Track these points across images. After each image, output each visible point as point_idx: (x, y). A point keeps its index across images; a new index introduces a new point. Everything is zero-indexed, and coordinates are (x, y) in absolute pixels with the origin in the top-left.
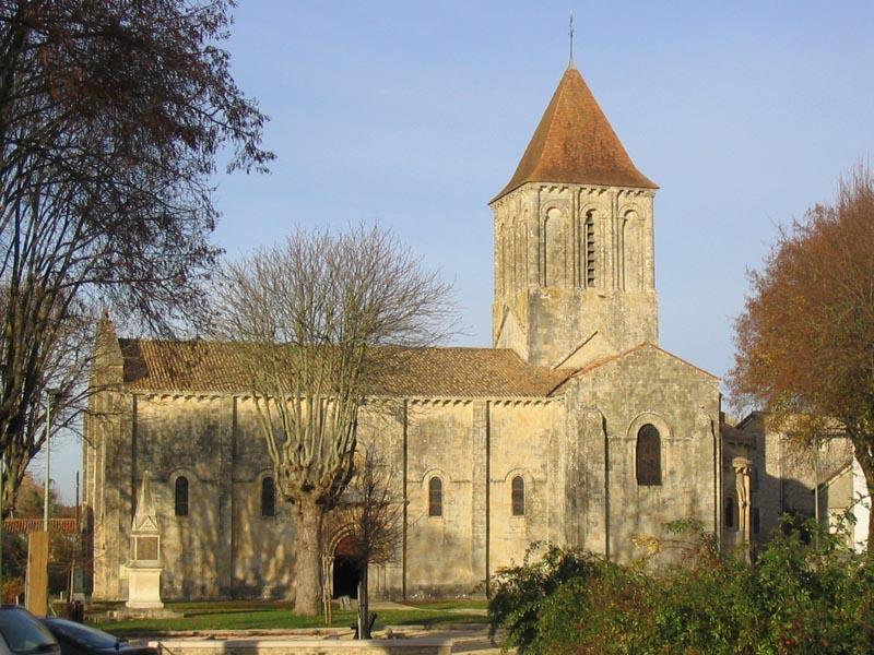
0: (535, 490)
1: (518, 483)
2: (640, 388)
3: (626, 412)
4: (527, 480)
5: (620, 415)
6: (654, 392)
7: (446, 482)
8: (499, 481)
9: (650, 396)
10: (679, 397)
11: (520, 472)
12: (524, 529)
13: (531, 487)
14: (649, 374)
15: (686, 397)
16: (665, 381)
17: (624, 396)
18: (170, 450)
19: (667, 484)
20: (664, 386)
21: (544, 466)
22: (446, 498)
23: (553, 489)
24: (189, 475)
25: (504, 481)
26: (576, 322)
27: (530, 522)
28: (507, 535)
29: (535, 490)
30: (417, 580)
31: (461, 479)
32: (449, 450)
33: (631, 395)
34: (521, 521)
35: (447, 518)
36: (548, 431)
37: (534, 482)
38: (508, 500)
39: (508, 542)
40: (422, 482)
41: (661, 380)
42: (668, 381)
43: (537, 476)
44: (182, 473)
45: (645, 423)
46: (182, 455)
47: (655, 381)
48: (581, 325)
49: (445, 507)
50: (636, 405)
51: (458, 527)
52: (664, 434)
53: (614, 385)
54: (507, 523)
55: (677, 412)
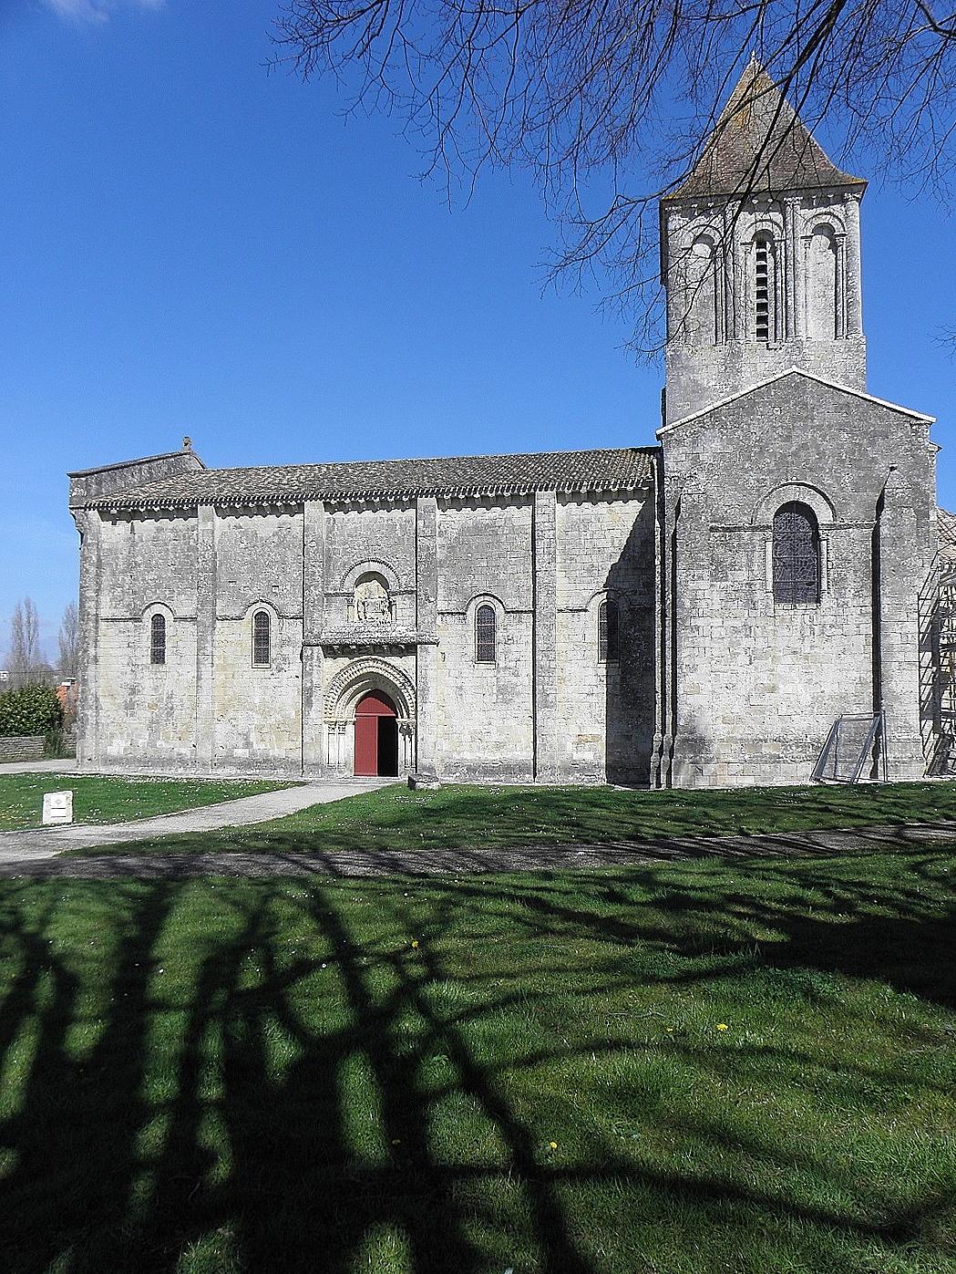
0: (632, 623)
2: (779, 443)
6: (804, 446)
7: (499, 611)
9: (795, 454)
13: (628, 616)
15: (864, 453)
19: (826, 600)
22: (499, 635)
24: (164, 611)
29: (632, 623)
40: (464, 614)
45: (786, 500)
46: (158, 586)
47: (804, 429)
49: (499, 649)
50: (771, 472)
52: (824, 515)
53: (730, 441)
54: (591, 671)
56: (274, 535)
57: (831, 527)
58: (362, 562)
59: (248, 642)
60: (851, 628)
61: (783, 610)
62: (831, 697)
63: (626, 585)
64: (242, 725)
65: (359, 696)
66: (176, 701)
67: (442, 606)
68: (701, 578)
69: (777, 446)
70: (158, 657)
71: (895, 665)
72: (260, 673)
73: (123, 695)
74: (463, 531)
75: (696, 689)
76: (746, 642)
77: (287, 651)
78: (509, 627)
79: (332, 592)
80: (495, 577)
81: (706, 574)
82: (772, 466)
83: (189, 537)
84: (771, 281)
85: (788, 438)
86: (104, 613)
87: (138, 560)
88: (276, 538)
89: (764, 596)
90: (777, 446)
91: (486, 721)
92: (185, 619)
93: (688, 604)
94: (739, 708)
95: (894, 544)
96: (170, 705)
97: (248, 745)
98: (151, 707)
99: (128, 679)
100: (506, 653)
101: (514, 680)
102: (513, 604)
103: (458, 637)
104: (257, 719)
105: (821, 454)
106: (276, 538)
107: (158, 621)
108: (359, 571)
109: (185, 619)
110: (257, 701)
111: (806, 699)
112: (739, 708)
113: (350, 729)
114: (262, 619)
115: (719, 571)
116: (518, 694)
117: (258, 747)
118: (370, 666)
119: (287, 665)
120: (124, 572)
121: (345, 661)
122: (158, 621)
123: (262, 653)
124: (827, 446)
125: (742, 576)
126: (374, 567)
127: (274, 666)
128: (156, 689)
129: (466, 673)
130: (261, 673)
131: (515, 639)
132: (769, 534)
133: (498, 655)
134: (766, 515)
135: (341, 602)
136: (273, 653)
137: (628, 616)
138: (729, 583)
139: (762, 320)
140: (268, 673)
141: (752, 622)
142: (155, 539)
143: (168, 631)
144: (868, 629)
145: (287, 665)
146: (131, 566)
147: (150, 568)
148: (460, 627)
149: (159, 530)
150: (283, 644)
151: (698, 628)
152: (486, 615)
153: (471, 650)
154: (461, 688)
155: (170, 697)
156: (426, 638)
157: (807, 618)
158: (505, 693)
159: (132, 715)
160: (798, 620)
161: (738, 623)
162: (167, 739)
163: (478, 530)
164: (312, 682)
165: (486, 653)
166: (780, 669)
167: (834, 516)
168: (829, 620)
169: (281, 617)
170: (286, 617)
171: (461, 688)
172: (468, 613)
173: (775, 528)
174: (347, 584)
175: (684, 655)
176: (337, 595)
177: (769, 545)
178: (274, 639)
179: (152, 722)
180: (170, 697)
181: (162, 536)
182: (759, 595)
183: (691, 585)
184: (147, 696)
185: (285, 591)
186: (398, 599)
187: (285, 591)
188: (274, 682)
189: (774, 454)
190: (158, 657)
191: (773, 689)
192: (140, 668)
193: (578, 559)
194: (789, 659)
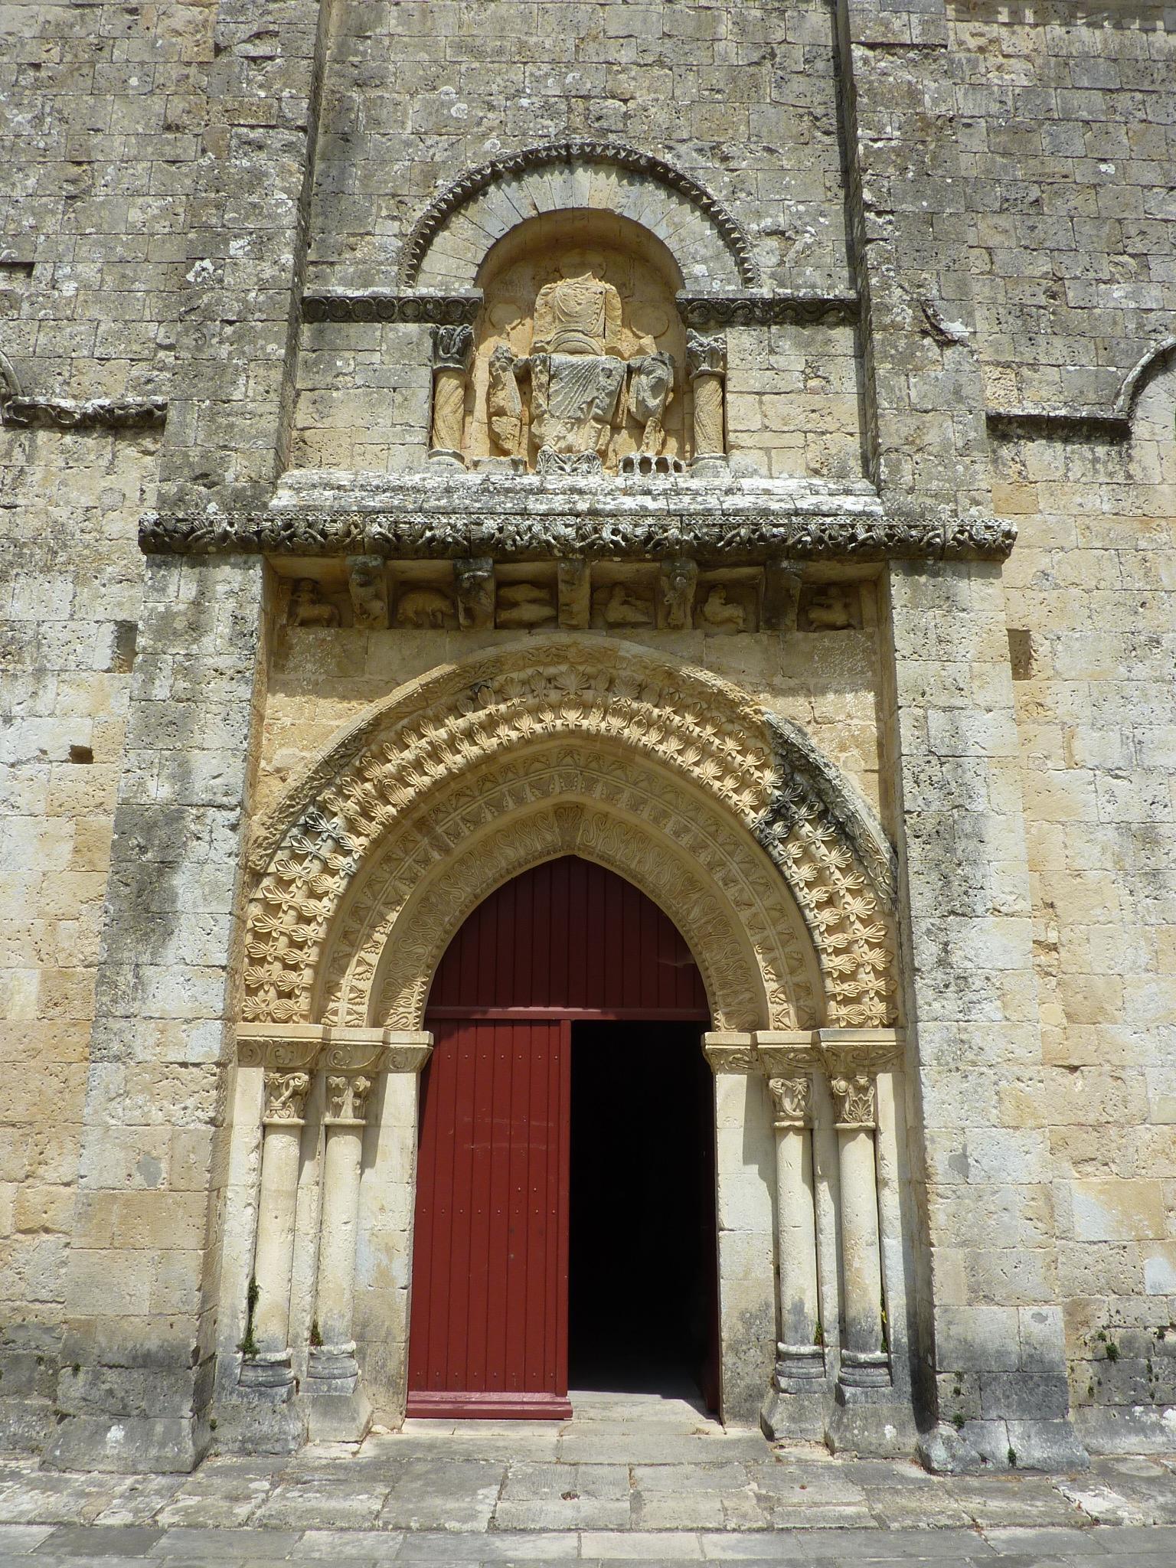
40: (1117, 432)
56: (42, 37)
145: (22, 688)
148: (1100, 501)
154: (1147, 836)
164: (183, 775)
170: (57, 420)
176: (379, 311)
186: (738, 341)
187: (69, 289)
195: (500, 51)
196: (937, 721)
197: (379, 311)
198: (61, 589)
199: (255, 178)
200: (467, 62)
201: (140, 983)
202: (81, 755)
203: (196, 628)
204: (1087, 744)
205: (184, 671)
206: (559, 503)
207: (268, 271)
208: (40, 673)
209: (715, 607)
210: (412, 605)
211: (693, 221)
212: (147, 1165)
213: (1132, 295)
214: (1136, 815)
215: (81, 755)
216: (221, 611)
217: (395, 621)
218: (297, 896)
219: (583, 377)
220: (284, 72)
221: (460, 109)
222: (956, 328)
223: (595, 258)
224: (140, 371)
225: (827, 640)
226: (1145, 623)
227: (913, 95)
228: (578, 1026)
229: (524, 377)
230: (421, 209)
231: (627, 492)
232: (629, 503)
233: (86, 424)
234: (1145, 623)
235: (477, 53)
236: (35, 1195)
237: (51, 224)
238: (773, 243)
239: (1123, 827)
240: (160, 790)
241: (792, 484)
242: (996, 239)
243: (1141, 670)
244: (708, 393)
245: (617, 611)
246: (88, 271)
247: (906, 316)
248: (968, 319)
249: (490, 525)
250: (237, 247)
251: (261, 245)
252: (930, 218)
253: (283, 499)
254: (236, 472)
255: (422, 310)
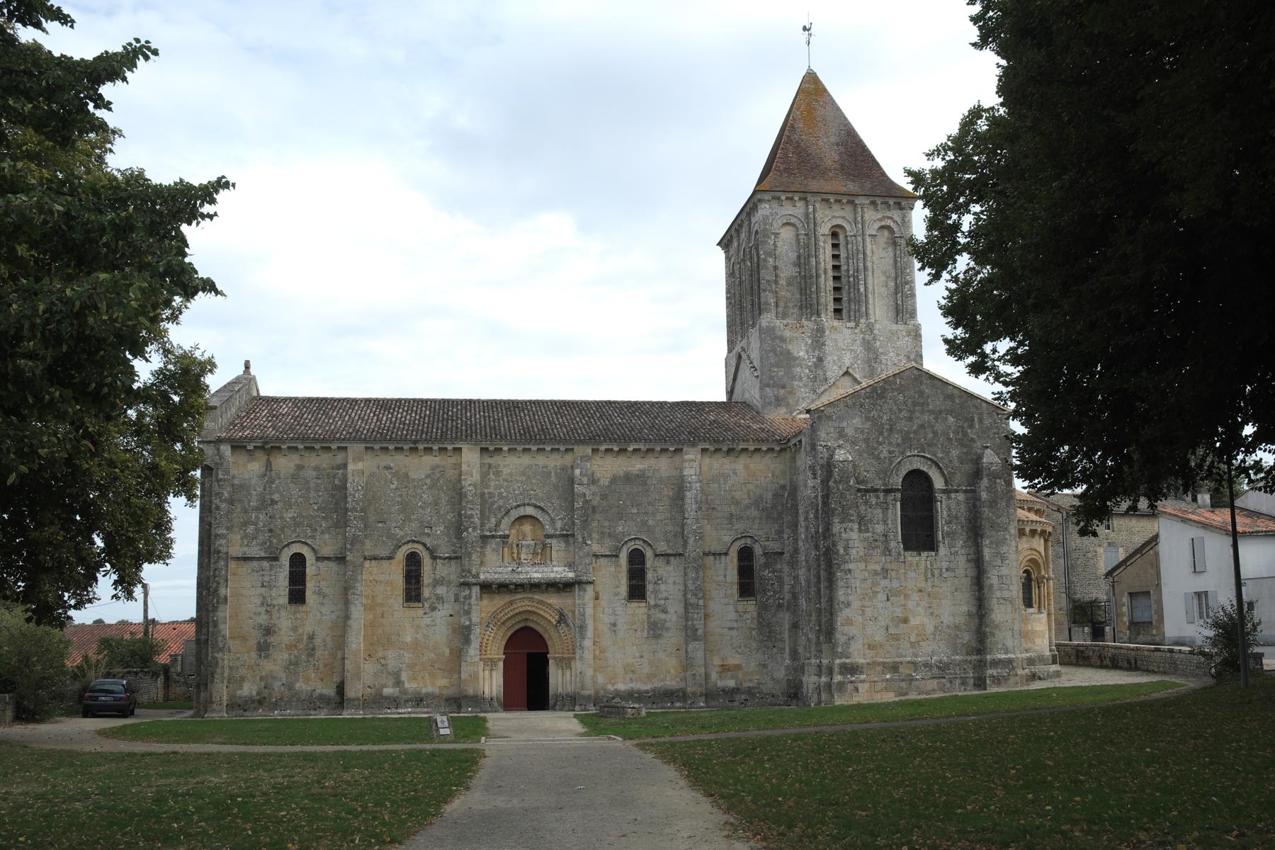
0: (766, 565)
1: (745, 555)
2: (903, 423)
3: (885, 454)
4: (758, 550)
5: (878, 458)
6: (922, 426)
7: (649, 554)
8: (720, 554)
9: (915, 432)
10: (956, 433)
11: (749, 541)
12: (755, 614)
13: (762, 560)
14: (915, 404)
15: (965, 434)
16: (937, 414)
17: (881, 433)
18: (281, 518)
19: (943, 550)
20: (936, 419)
21: (780, 532)
22: (650, 576)
23: (793, 564)
24: (306, 551)
25: (726, 554)
26: (820, 360)
27: (763, 607)
28: (735, 625)
29: (766, 565)
30: (613, 684)
31: (669, 551)
32: (654, 514)
33: (891, 430)
34: (751, 606)
35: (652, 602)
36: (783, 487)
37: (765, 554)
38: (733, 575)
39: (734, 633)
40: (617, 556)
41: (931, 412)
42: (940, 412)
43: (773, 546)
44: (297, 548)
45: (911, 469)
46: (297, 525)
47: (922, 412)
48: (825, 363)
49: (650, 587)
50: (898, 445)
51: (665, 611)
52: (938, 483)
53: (867, 419)
54: (731, 608)
55: (955, 453)
57: (944, 491)
58: (518, 506)
59: (399, 581)
60: (960, 572)
61: (911, 557)
62: (948, 627)
63: (761, 533)
64: (392, 664)
65: (509, 634)
66: (318, 641)
67: (596, 548)
68: (852, 530)
69: (902, 425)
70: (297, 596)
71: (995, 601)
72: (411, 613)
73: (255, 637)
74: (614, 480)
75: (849, 622)
76: (884, 583)
77: (441, 590)
78: (658, 569)
79: (488, 534)
80: (644, 523)
81: (856, 526)
82: (899, 441)
83: (334, 477)
84: (844, 268)
85: (910, 419)
86: (236, 551)
87: (276, 497)
88: (428, 481)
89: (896, 543)
90: (902, 425)
91: (637, 655)
92: (328, 559)
93: (842, 551)
94: (879, 637)
95: (991, 506)
96: (311, 646)
97: (398, 683)
98: (290, 647)
99: (263, 619)
100: (656, 592)
101: (663, 616)
102: (662, 547)
103: (613, 578)
104: (408, 657)
105: (935, 433)
106: (428, 481)
107: (298, 562)
108: (515, 514)
109: (328, 559)
110: (408, 639)
111: (930, 628)
112: (879, 637)
113: (501, 664)
114: (413, 562)
115: (863, 523)
116: (667, 629)
117: (411, 686)
118: (523, 603)
119: (441, 605)
120: (258, 509)
121: (500, 601)
122: (298, 562)
123: (413, 592)
124: (939, 427)
125: (880, 528)
126: (530, 511)
127: (427, 605)
128: (294, 629)
129: (619, 610)
130: (417, 612)
131: (664, 579)
132: (899, 495)
133: (648, 594)
134: (897, 481)
135: (497, 544)
136: (426, 592)
137: (762, 560)
138: (870, 534)
139: (837, 300)
140: (421, 612)
141: (888, 566)
142: (294, 477)
143: (310, 569)
144: (972, 572)
145: (441, 605)
146: (264, 504)
147: (288, 506)
149: (300, 467)
150: (437, 583)
151: (850, 571)
152: (637, 560)
153: (624, 589)
154: (614, 625)
155: (311, 637)
156: (584, 578)
157: (928, 563)
158: (655, 630)
159: (265, 657)
160: (922, 566)
161: (878, 568)
162: (307, 680)
163: (628, 478)
164: (470, 620)
165: (637, 591)
166: (910, 604)
167: (946, 483)
168: (945, 565)
169: (434, 558)
170: (440, 558)
171: (614, 625)
172: (621, 555)
173: (903, 491)
174: (503, 526)
175: (841, 594)
176: (493, 537)
177: (898, 504)
178: (427, 578)
179: (291, 664)
180: (311, 637)
181: (303, 474)
182: (893, 544)
183: (844, 535)
184: (285, 634)
185: (439, 532)
186: (554, 542)
187: (439, 532)
188: (427, 620)
189: (901, 431)
190: (297, 596)
191: (906, 621)
192: (276, 608)
193: (719, 508)
194: (915, 597)
195: (512, 481)
196: (581, 609)
197: (493, 537)
198: (444, 588)
199: (471, 516)
200: (506, 484)
201: (467, 652)
202: (451, 615)
203: (470, 598)
204: (606, 610)
205: (469, 604)
206: (525, 576)
207: (476, 534)
208: (443, 603)
209: (549, 589)
210: (501, 589)
211: (546, 517)
212: (471, 676)
213: (623, 529)
214: (613, 622)
215: (451, 615)
216: (474, 594)
217: (498, 593)
218: (487, 637)
219: (528, 546)
220: (475, 493)
221: (505, 494)
222: (589, 542)
223: (529, 520)
224: (453, 548)
225: (567, 594)
226: (618, 590)
227: (585, 495)
228: (528, 654)
229: (518, 545)
230: (499, 516)
231: (536, 572)
232: (536, 575)
233: (445, 558)
234: (618, 590)
235: (508, 482)
236: (452, 680)
237: (434, 519)
238: (560, 521)
239: (611, 624)
240: (467, 623)
241: (560, 569)
242: (599, 518)
243: (616, 598)
244: (549, 549)
245: (534, 590)
246: (442, 528)
247: (581, 540)
248: (591, 540)
249: (514, 580)
250: (470, 530)
251: (475, 529)
252: (586, 521)
253: (482, 577)
254: (474, 572)
255: (500, 537)
